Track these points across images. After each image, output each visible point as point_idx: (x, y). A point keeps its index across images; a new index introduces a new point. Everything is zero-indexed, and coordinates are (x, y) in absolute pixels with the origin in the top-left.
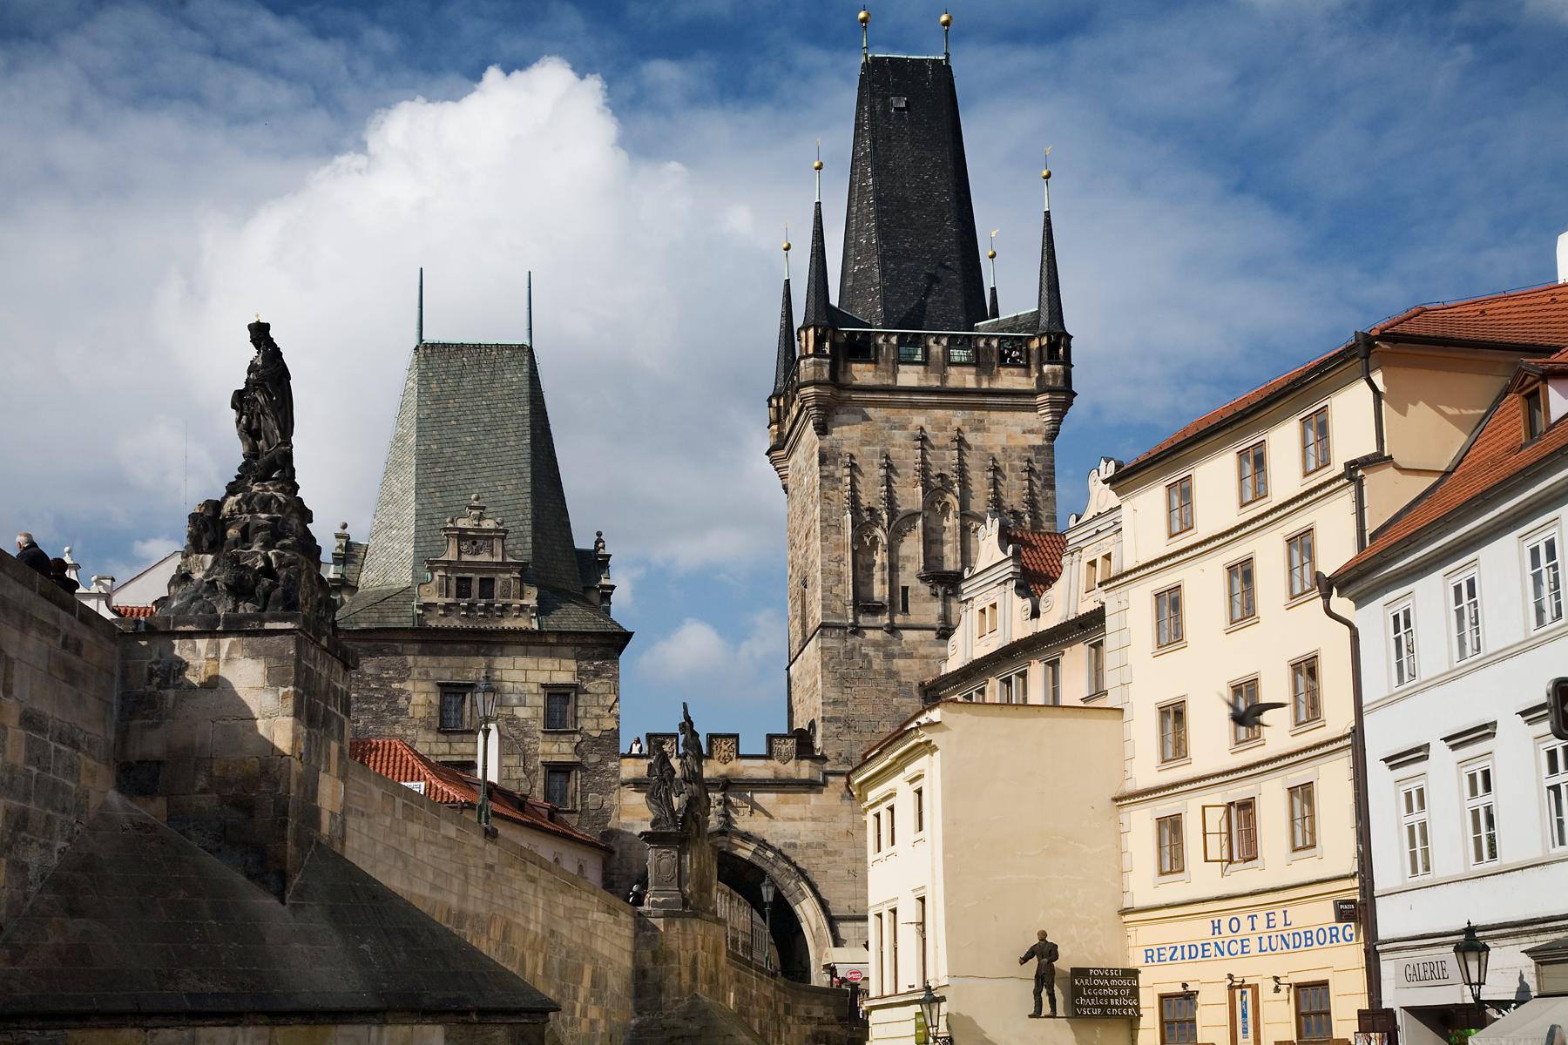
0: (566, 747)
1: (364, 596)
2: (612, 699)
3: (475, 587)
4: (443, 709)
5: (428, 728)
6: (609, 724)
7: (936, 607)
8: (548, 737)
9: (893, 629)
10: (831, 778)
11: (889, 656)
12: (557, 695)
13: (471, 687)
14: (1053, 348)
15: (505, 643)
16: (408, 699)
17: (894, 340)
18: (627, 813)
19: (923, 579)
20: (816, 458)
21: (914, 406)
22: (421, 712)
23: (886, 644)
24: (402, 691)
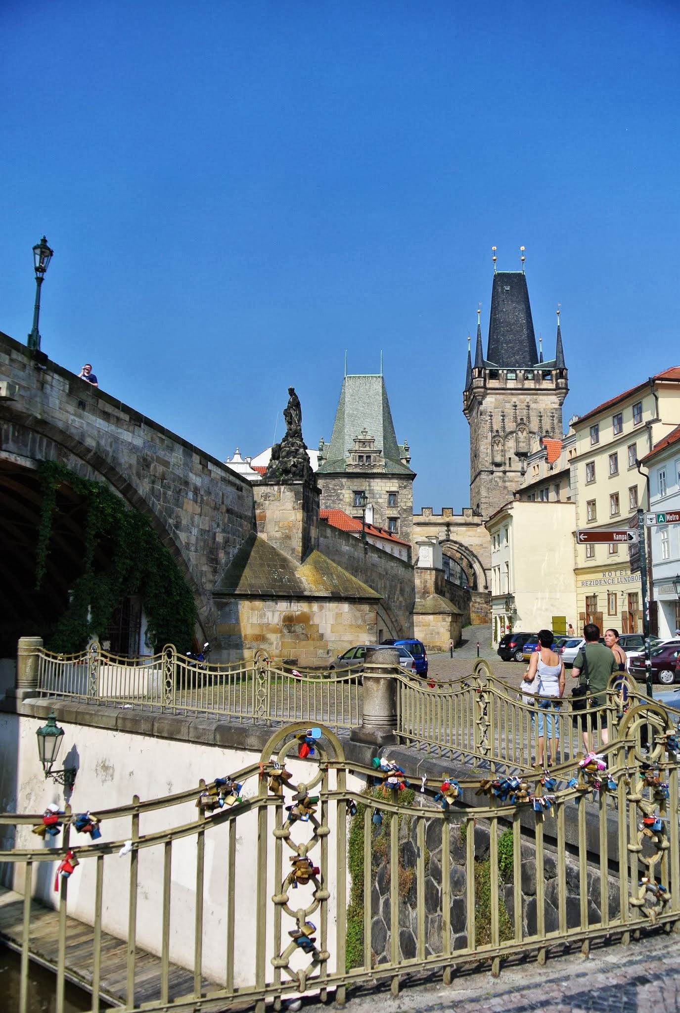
0: (395, 512)
2: (410, 496)
3: (365, 458)
5: (350, 505)
6: (410, 504)
9: (505, 472)
11: (504, 481)
12: (392, 494)
14: (561, 373)
17: (505, 372)
21: (512, 394)
22: (347, 500)
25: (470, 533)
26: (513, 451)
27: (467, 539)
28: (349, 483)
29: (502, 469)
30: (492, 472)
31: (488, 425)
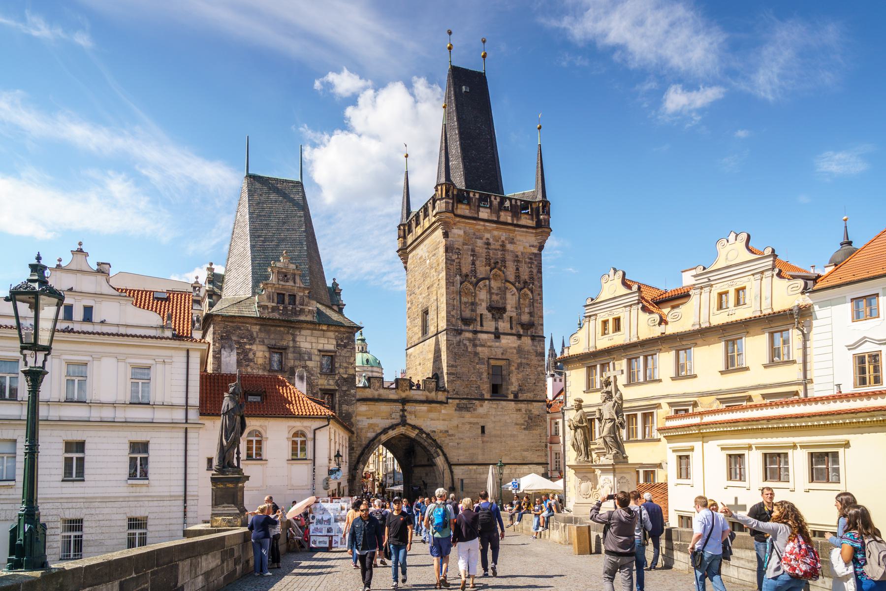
0: (331, 382)
1: (227, 299)
4: (270, 359)
5: (264, 369)
7: (493, 324)
8: (323, 376)
10: (450, 401)
11: (475, 346)
13: (285, 348)
15: (302, 328)
16: (254, 354)
18: (360, 415)
19: (489, 311)
20: (442, 250)
22: (260, 361)
23: (474, 339)
24: (250, 350)
25: (433, 415)
26: (484, 305)
27: (429, 423)
28: (262, 335)
29: (471, 328)
30: (459, 332)
31: (454, 268)
